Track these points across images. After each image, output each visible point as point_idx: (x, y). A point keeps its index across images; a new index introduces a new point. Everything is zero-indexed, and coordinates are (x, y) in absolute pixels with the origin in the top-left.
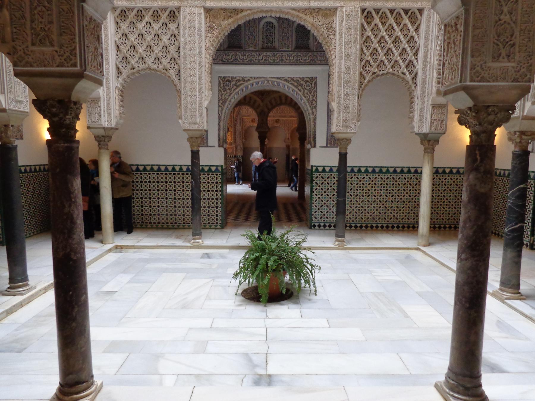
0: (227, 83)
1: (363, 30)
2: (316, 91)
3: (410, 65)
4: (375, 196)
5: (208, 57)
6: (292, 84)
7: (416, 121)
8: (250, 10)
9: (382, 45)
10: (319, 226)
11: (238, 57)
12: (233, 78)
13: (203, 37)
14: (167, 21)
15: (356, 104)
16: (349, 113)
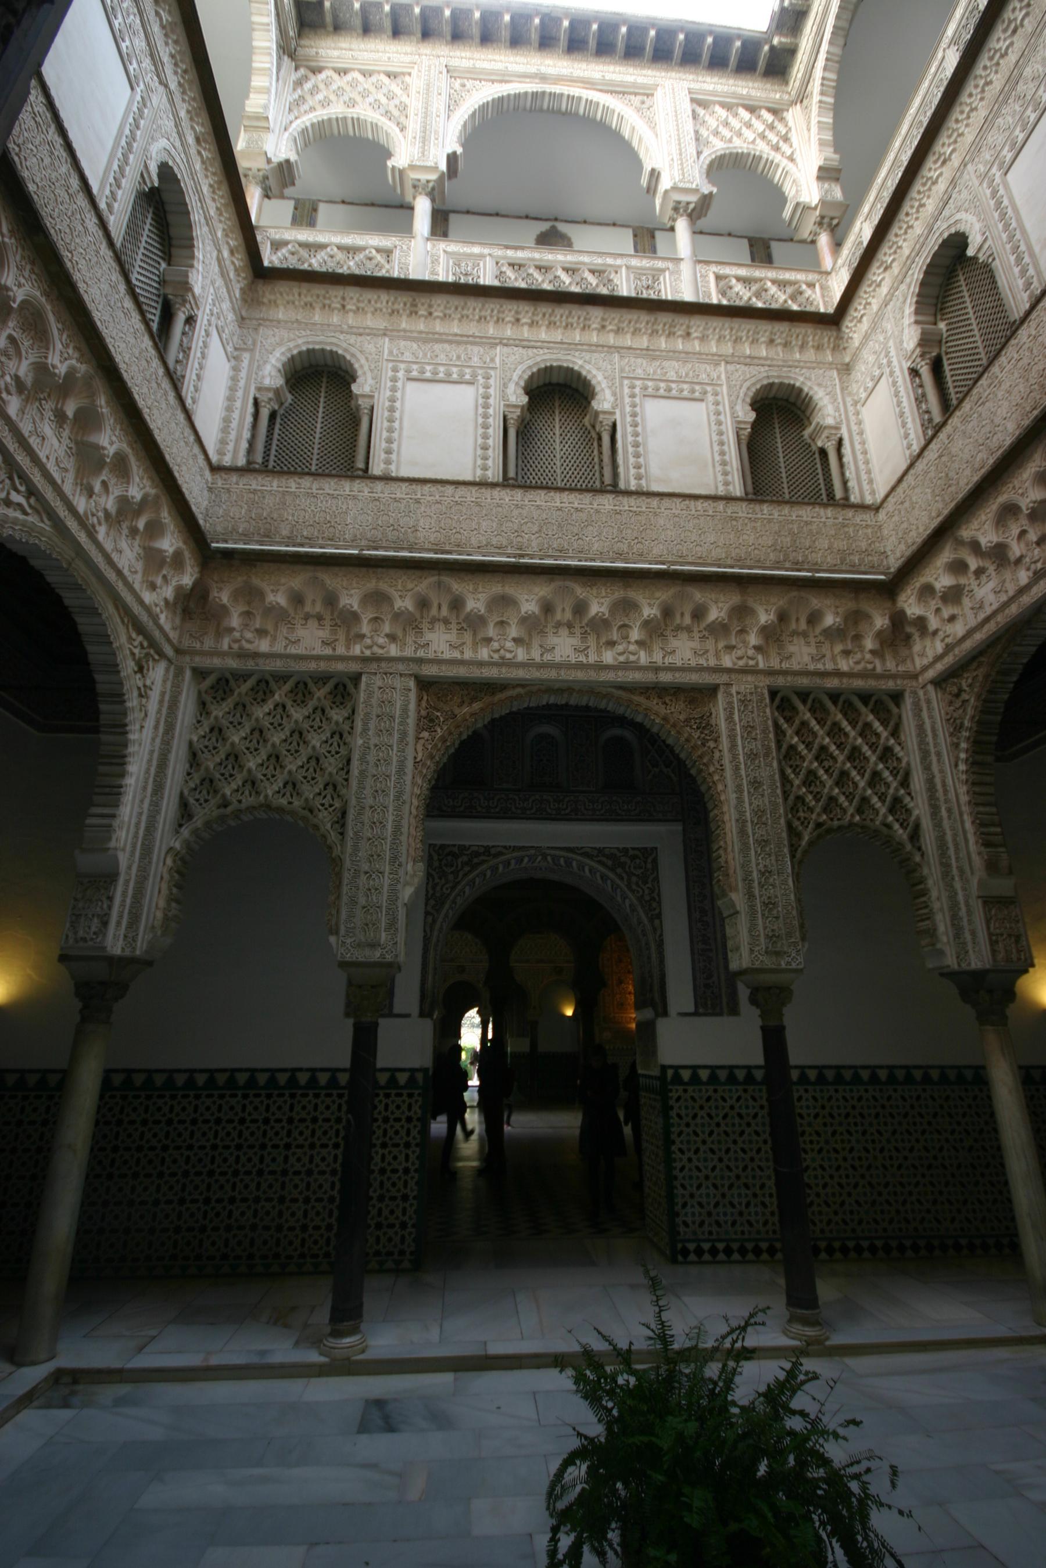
0: (449, 858)
2: (656, 879)
3: (896, 806)
4: (836, 1151)
5: (420, 782)
6: (599, 862)
7: (945, 939)
8: (523, 686)
10: (699, 1252)
12: (463, 848)
13: (411, 739)
14: (327, 704)
16: (777, 918)
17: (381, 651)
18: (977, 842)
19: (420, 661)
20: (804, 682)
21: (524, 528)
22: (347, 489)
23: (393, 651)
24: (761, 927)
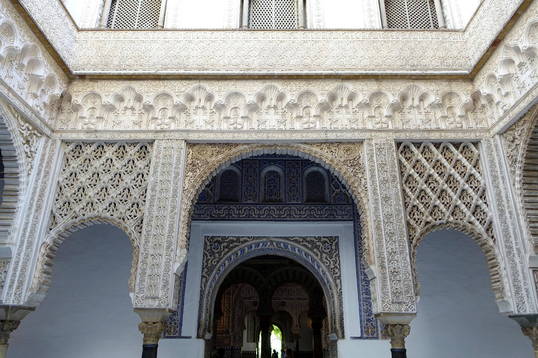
0: (216, 244)
1: (401, 168)
2: (338, 255)
5: (186, 202)
7: (509, 294)
9: (432, 185)
11: (231, 212)
12: (224, 238)
13: (181, 177)
15: (409, 267)
17: (166, 127)
18: (528, 233)
19: (188, 131)
20: (417, 136)
21: (250, 53)
22: (152, 37)
23: (173, 127)
24: (389, 287)
